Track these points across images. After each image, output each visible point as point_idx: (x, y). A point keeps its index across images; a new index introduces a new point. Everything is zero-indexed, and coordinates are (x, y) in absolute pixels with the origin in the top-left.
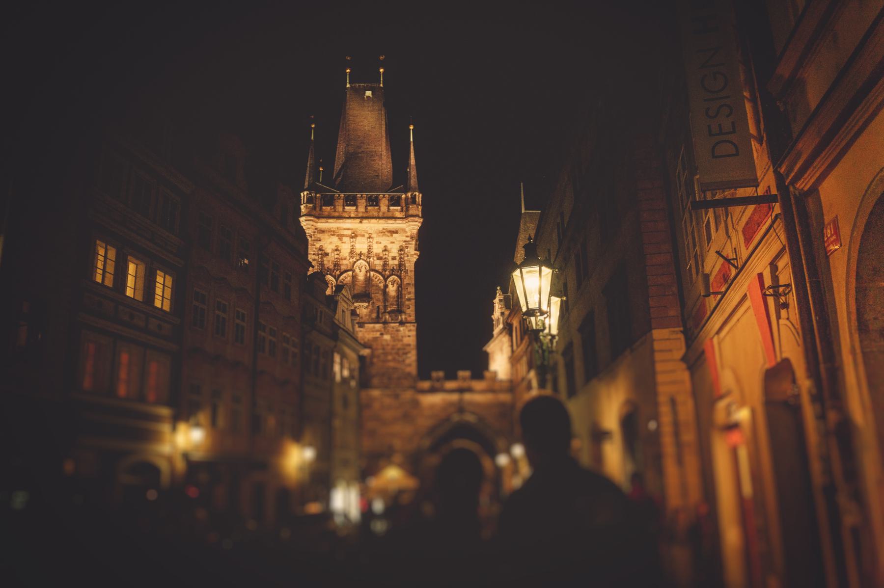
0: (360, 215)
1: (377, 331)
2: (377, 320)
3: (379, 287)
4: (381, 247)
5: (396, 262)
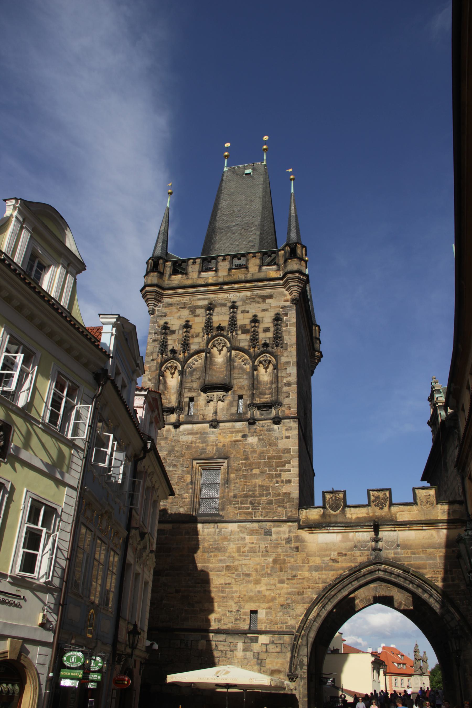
0: (221, 280)
1: (238, 432)
2: (239, 418)
3: (244, 370)
4: (250, 315)
5: (270, 335)
